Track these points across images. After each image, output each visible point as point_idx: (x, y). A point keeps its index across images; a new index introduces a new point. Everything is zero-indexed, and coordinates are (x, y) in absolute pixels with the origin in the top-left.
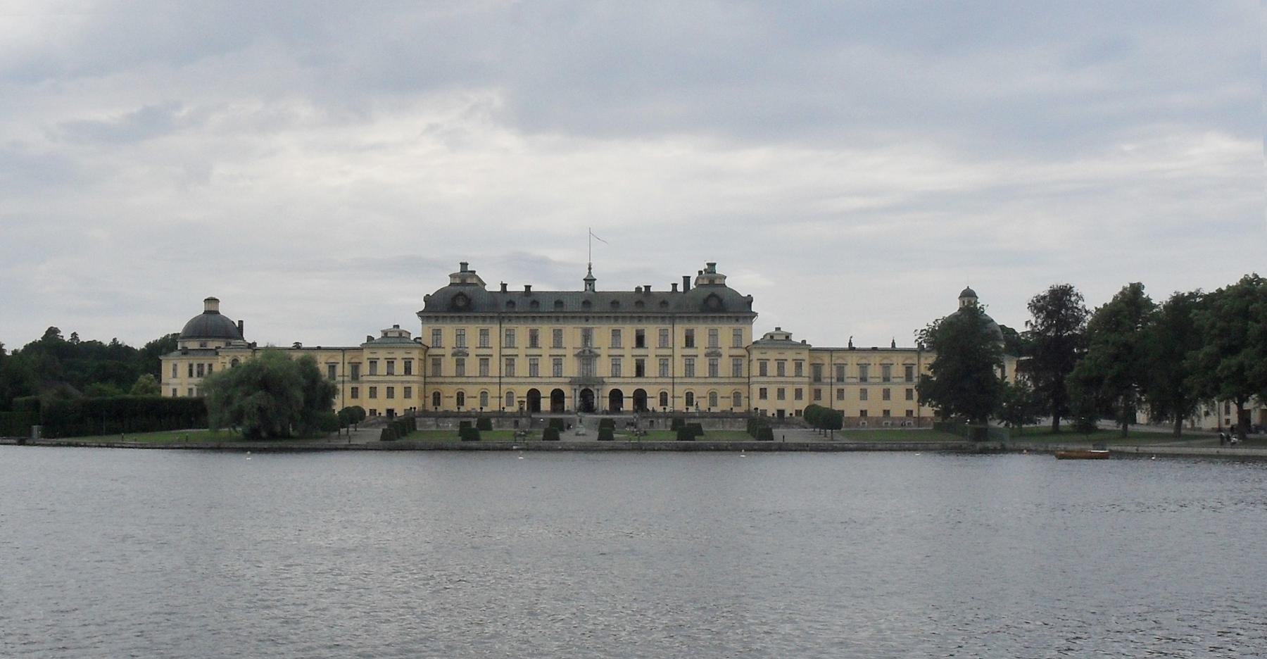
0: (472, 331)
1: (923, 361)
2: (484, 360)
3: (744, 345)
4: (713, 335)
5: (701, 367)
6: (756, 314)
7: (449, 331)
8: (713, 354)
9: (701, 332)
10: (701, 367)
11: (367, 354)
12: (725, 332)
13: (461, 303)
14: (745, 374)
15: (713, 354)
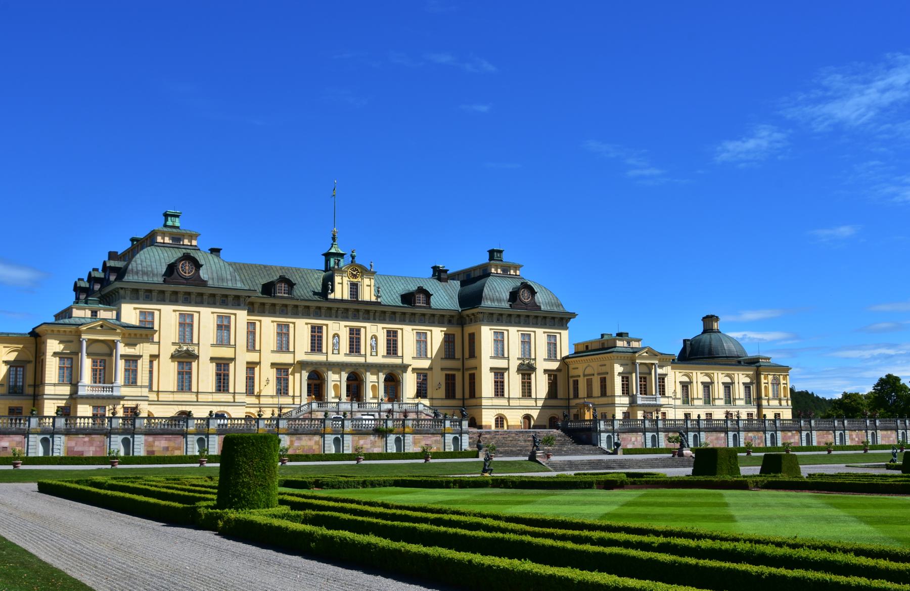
0: (206, 318)
1: (763, 381)
2: (222, 366)
3: (559, 358)
4: (526, 341)
5: (514, 383)
6: (573, 315)
7: (167, 317)
8: (527, 370)
9: (514, 334)
10: (514, 383)
11: (53, 346)
12: (540, 336)
13: (186, 270)
14: (561, 394)
15: (527, 370)
